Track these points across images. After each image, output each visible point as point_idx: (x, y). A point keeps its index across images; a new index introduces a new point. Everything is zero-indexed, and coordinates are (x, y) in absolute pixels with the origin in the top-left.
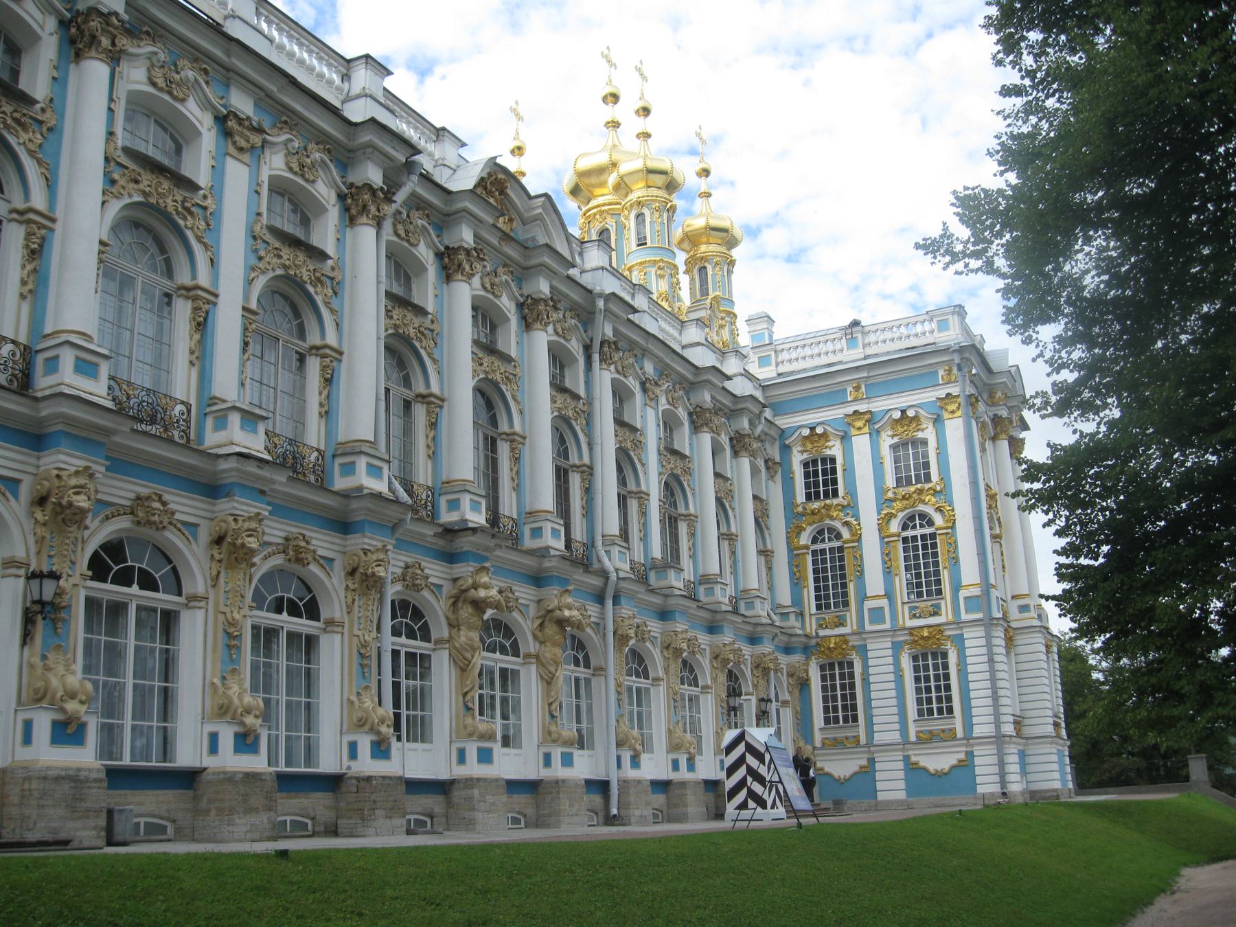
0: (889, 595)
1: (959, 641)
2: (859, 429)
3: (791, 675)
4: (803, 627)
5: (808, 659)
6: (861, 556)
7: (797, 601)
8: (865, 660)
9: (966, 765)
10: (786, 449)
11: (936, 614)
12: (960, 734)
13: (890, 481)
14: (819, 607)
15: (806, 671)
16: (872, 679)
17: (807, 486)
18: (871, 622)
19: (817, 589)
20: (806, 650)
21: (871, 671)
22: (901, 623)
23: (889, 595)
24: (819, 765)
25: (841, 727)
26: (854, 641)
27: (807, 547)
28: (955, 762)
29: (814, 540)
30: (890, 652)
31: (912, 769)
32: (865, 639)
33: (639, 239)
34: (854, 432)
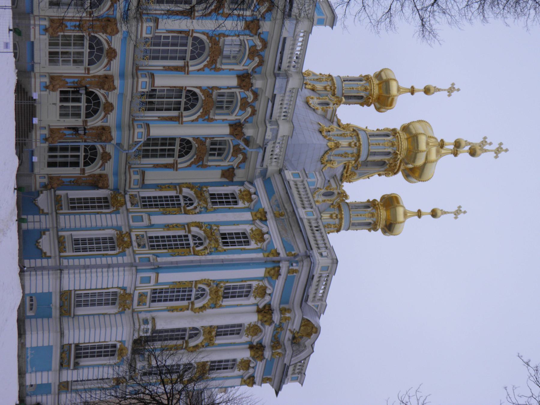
0: (151, 226)
1: (122, 253)
2: (256, 215)
3: (100, 176)
6: (175, 214)
8: (110, 213)
9: (42, 255)
10: (242, 183)
11: (139, 245)
12: (62, 254)
13: (224, 229)
20: (116, 190)
21: (103, 216)
22: (133, 230)
23: (151, 226)
24: (44, 192)
25: (68, 205)
28: (45, 251)
30: (115, 223)
31: (41, 232)
32: (123, 213)
34: (254, 213)
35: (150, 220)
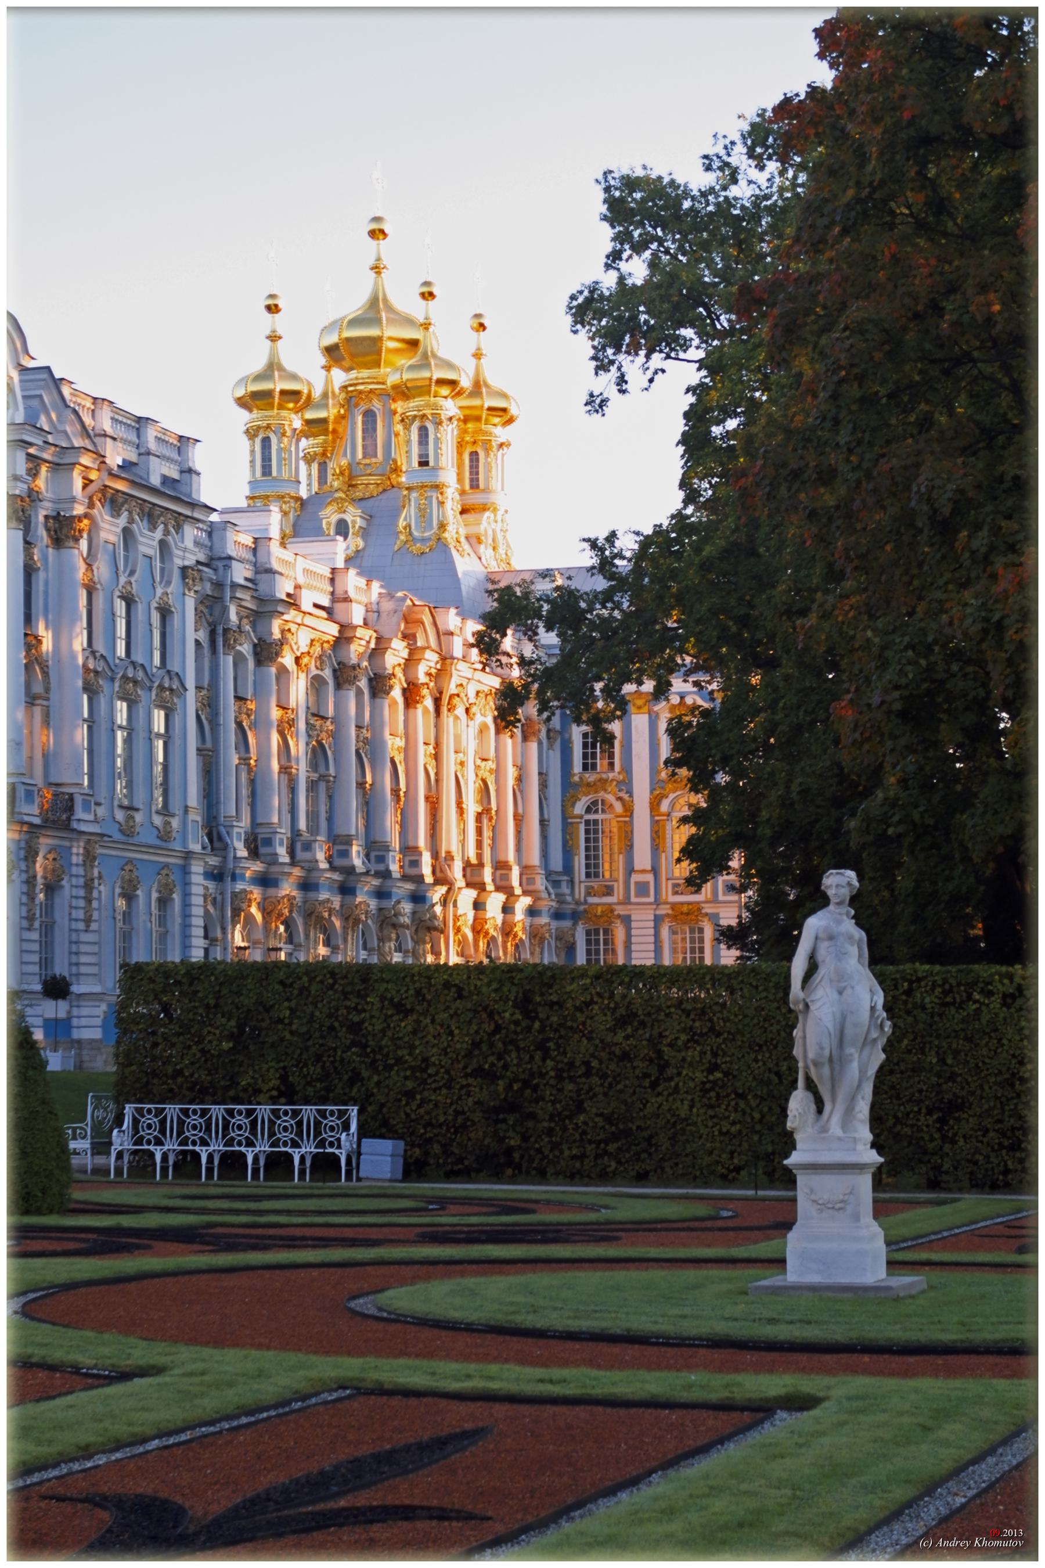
0: (655, 870)
2: (639, 708)
3: (558, 938)
4: (572, 893)
5: (575, 924)
7: (568, 868)
14: (588, 875)
15: (573, 935)
16: (633, 947)
17: (585, 756)
18: (637, 896)
19: (587, 857)
21: (633, 940)
26: (620, 910)
27: (581, 817)
29: (588, 810)
30: (652, 924)
33: (420, 456)
35: (643, 871)
